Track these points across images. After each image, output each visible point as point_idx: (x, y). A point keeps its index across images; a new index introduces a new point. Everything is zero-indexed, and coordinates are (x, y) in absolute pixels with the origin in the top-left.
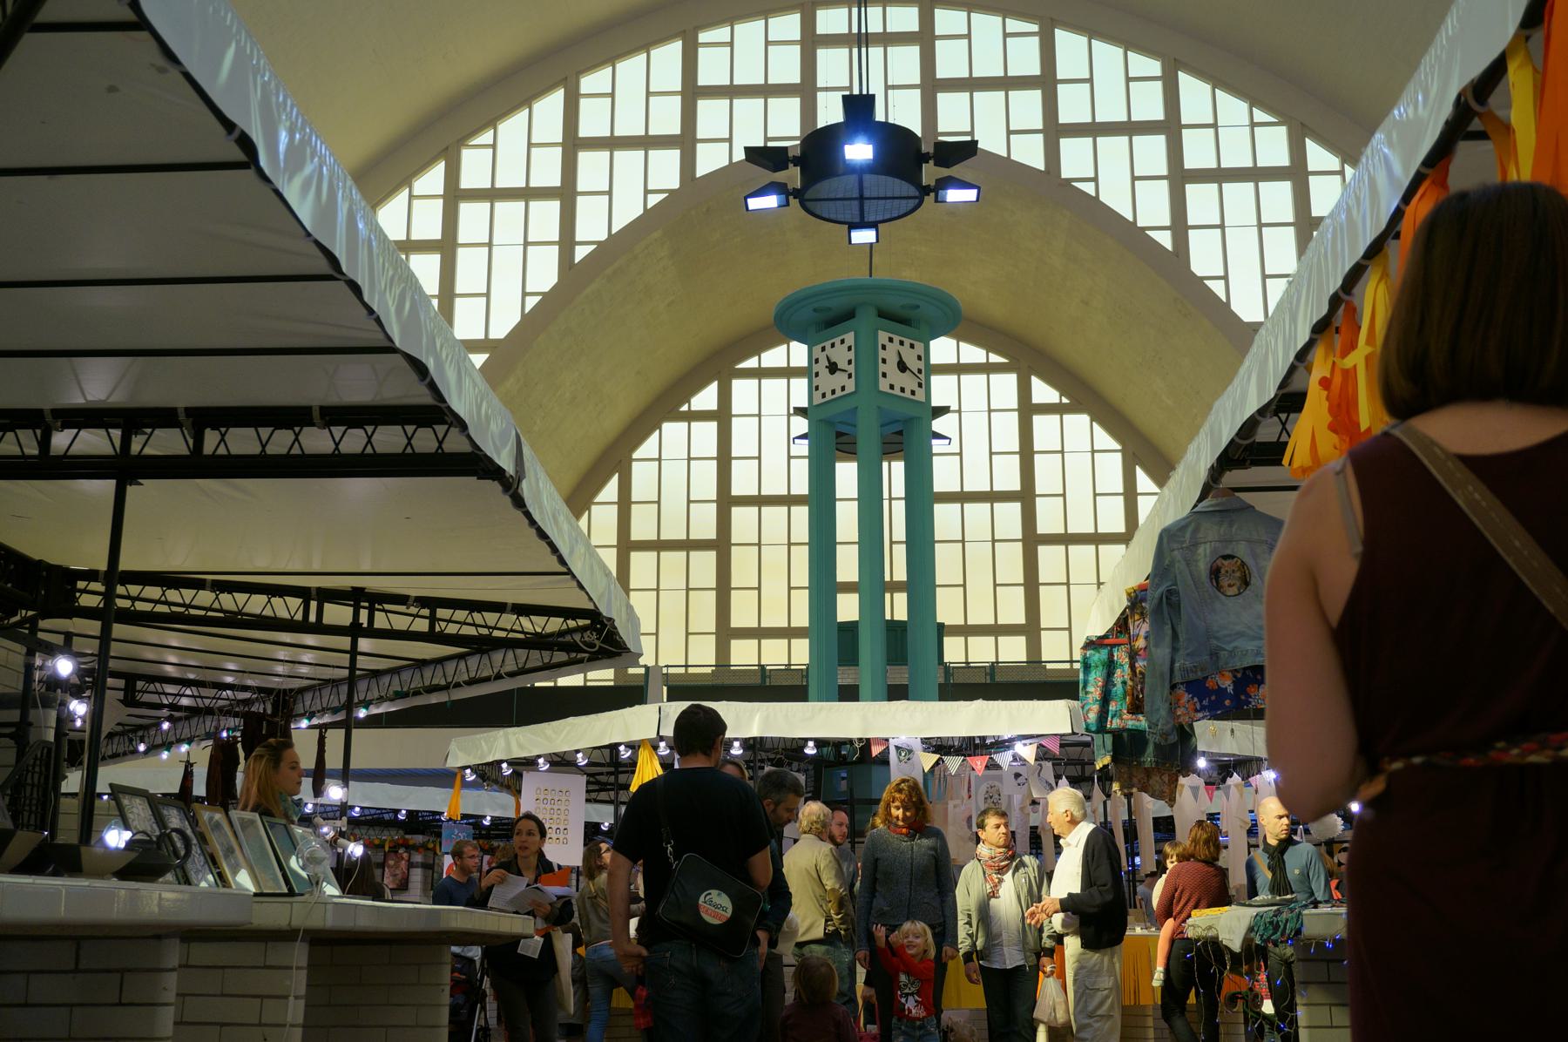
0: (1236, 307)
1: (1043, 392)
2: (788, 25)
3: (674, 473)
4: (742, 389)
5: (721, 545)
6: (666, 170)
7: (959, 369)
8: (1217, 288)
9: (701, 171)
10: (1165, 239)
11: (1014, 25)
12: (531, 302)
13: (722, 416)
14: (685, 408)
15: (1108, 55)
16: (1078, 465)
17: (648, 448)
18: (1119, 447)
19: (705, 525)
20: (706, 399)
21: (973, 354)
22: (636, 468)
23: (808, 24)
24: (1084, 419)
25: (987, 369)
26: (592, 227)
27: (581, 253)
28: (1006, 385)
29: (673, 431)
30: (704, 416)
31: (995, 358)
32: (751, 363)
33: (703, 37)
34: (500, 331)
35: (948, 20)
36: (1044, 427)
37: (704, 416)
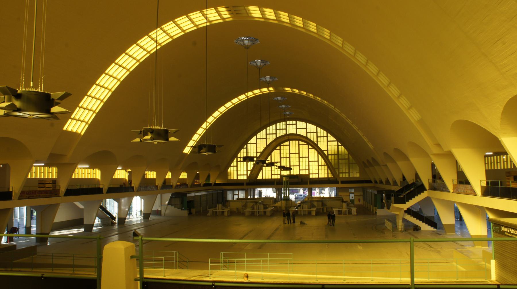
0: (322, 149)
1: (310, 147)
2: (284, 123)
3: (276, 155)
6: (274, 137)
7: (302, 145)
8: (320, 147)
9: (277, 137)
10: (316, 143)
11: (304, 123)
12: (264, 148)
13: (280, 149)
15: (312, 125)
16: (313, 154)
17: (273, 153)
18: (317, 152)
20: (278, 148)
21: (304, 143)
22: (272, 155)
23: (286, 123)
24: (314, 149)
25: (305, 145)
26: (268, 142)
27: (268, 144)
28: (307, 146)
29: (275, 151)
31: (306, 144)
32: (282, 144)
33: (277, 124)
35: (298, 122)
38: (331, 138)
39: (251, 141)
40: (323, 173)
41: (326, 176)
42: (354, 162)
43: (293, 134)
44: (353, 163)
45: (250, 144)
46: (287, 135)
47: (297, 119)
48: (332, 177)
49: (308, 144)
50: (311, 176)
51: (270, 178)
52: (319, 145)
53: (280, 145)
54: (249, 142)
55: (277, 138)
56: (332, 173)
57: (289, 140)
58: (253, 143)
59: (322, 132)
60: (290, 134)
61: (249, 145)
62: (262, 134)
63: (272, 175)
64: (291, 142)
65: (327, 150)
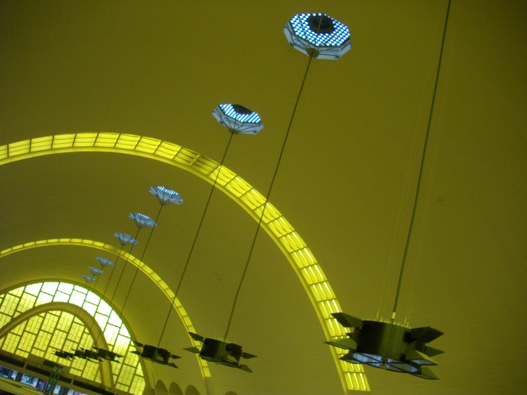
1: (87, 331)
2: (71, 286)
3: (35, 323)
4: (48, 315)
5: (37, 335)
7: (77, 323)
10: (103, 330)
12: (28, 309)
13: (44, 318)
14: (39, 315)
17: (32, 318)
19: (36, 332)
20: (43, 315)
21: (80, 322)
25: (80, 324)
27: (36, 305)
29: (37, 317)
30: (42, 317)
31: (83, 324)
32: (51, 312)
34: (23, 311)
36: (85, 336)
37: (42, 317)
38: (124, 331)
39: (16, 292)
40: (89, 374)
41: (92, 379)
42: (142, 374)
43: (77, 307)
44: (139, 376)
45: (12, 295)
46: (68, 304)
47: (89, 288)
48: (100, 382)
49: (86, 326)
50: (72, 371)
51: (12, 351)
52: (106, 335)
53: (46, 311)
54: (11, 292)
55: (52, 303)
56: (102, 378)
57: (62, 310)
58: (16, 296)
59: (116, 319)
60: (73, 306)
61: (8, 296)
62: (33, 288)
63: (17, 348)
64: (64, 313)
65: (113, 346)
